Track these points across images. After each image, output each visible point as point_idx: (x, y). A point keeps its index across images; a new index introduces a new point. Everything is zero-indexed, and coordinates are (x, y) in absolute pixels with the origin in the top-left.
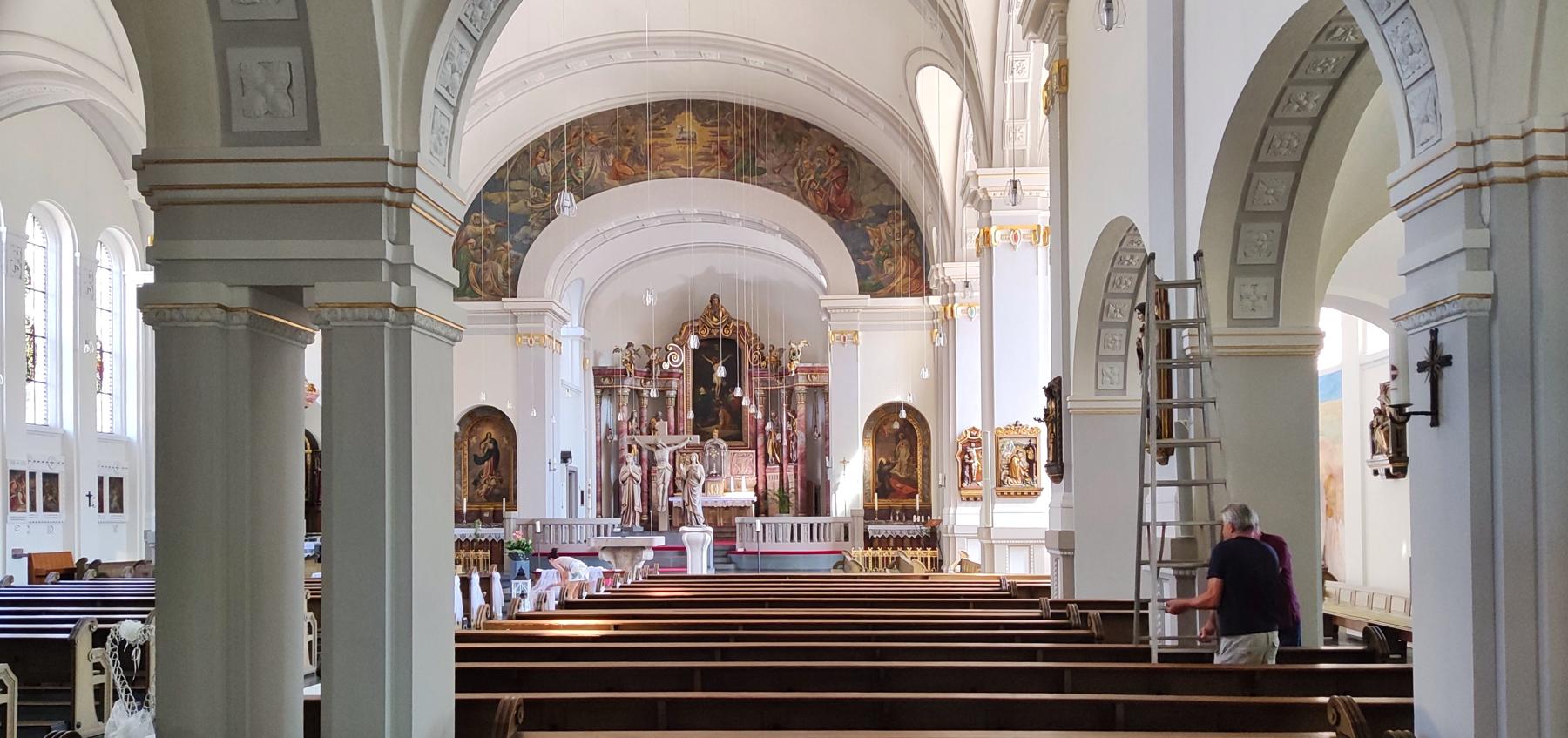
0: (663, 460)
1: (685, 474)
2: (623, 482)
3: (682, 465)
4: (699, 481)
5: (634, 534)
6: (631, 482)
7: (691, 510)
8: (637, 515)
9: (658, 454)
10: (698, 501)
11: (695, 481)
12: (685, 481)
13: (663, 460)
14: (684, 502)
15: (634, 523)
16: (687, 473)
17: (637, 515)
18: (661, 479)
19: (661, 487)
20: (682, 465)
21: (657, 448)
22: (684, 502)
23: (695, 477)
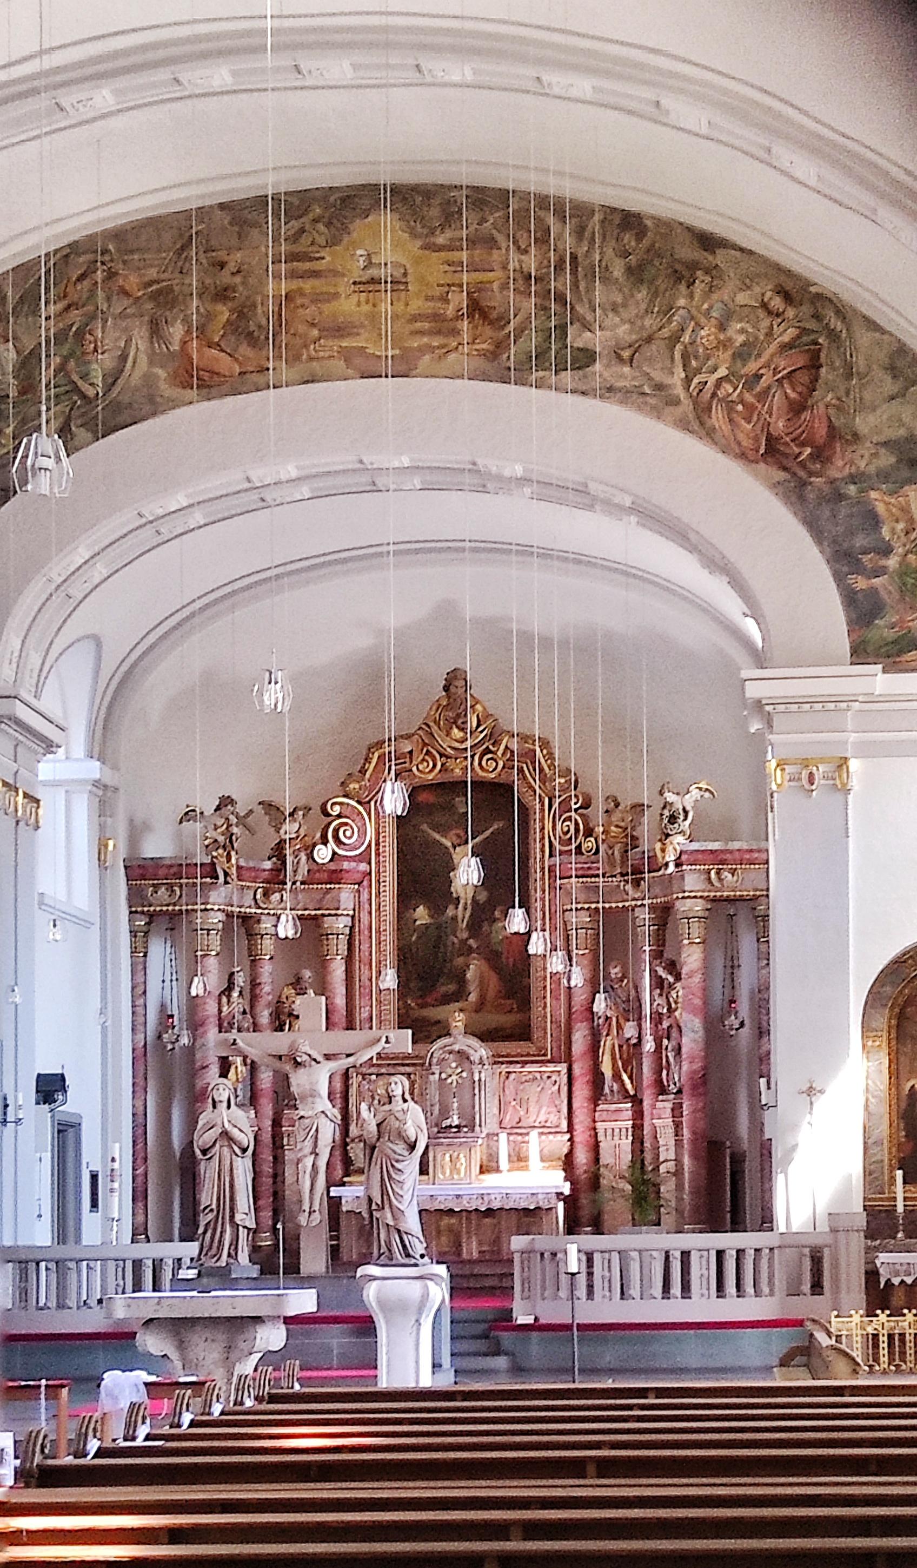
0: (313, 1094)
1: (373, 1128)
2: (204, 1152)
3: (364, 1106)
4: (412, 1147)
5: (233, 1284)
6: (226, 1150)
7: (391, 1223)
8: (243, 1233)
9: (299, 1081)
10: (407, 1197)
11: (400, 1148)
12: (373, 1148)
13: (313, 1094)
14: (370, 1200)
15: (233, 1255)
16: (378, 1125)
17: (243, 1233)
18: (308, 1144)
19: (309, 1161)
20: (364, 1106)
21: (297, 1064)
22: (370, 1200)
23: (401, 1135)
